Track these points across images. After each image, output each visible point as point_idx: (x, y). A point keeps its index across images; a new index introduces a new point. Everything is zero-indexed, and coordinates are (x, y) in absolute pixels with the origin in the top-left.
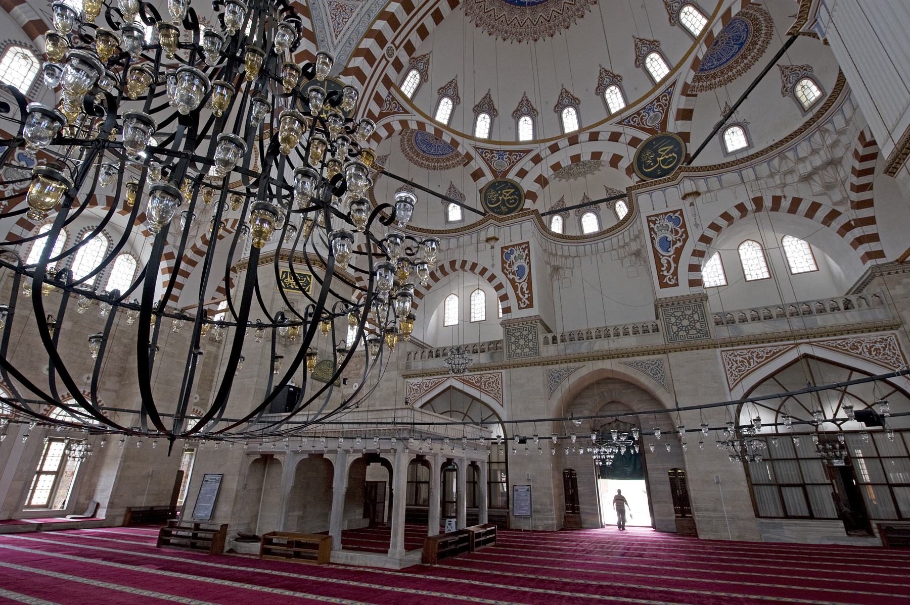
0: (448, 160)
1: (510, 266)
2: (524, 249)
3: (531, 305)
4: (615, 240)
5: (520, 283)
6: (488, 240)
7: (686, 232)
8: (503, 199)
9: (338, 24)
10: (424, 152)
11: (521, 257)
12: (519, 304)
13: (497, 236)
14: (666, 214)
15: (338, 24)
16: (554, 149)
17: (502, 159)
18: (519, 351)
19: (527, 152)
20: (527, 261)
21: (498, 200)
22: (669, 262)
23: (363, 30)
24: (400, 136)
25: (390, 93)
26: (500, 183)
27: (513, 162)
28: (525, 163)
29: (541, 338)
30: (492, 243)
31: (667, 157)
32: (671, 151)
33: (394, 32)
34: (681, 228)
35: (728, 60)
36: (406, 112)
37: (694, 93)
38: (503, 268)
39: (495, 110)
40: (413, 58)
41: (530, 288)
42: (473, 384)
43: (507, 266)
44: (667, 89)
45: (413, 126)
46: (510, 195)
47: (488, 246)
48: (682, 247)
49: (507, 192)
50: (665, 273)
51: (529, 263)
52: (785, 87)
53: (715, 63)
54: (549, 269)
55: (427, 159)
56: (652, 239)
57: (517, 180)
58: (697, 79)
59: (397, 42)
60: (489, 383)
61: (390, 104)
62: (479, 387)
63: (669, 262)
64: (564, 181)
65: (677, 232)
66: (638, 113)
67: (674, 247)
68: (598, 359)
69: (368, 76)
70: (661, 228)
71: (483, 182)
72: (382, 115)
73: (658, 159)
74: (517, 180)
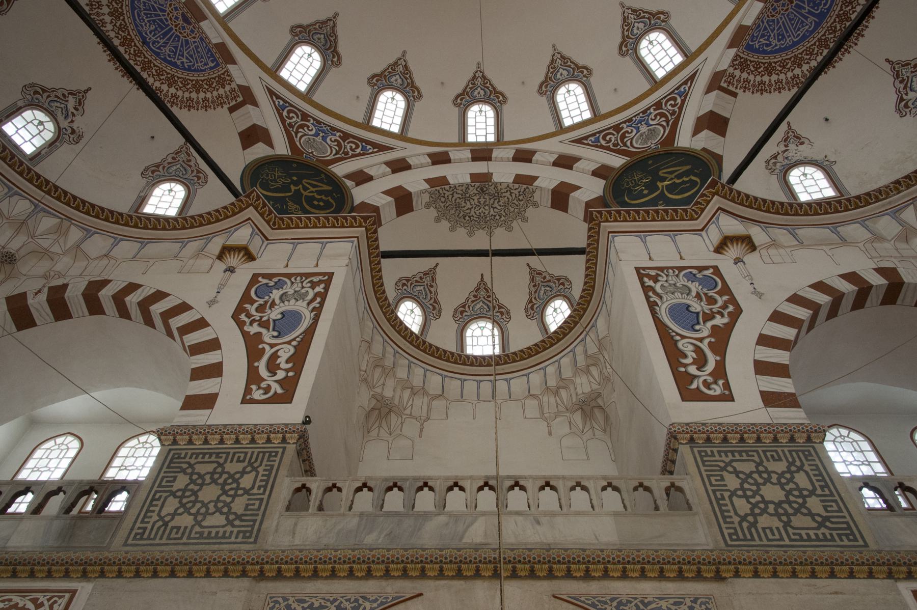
0: (197, 87)
1: (261, 309)
2: (313, 285)
3: (286, 397)
4: (536, 378)
5: (272, 346)
7: (733, 301)
8: (298, 192)
10: (145, 42)
11: (298, 296)
12: (248, 391)
13: (253, 249)
14: (681, 269)
16: (440, 159)
17: (324, 138)
18: (185, 521)
19: (382, 148)
20: (315, 304)
22: (698, 350)
27: (347, 153)
28: (372, 163)
29: (285, 486)
31: (678, 181)
32: (686, 173)
34: (721, 293)
35: (795, 44)
37: (731, 88)
39: (336, 53)
41: (299, 359)
43: (252, 309)
44: (677, 88)
47: (220, 266)
48: (730, 326)
50: (693, 370)
51: (318, 312)
52: (902, 100)
53: (774, 42)
54: (364, 399)
56: (652, 306)
58: (740, 63)
63: (698, 350)
64: (445, 224)
65: (711, 301)
66: (617, 128)
67: (709, 324)
68: (477, 575)
70: (672, 289)
71: (259, 151)
73: (660, 184)
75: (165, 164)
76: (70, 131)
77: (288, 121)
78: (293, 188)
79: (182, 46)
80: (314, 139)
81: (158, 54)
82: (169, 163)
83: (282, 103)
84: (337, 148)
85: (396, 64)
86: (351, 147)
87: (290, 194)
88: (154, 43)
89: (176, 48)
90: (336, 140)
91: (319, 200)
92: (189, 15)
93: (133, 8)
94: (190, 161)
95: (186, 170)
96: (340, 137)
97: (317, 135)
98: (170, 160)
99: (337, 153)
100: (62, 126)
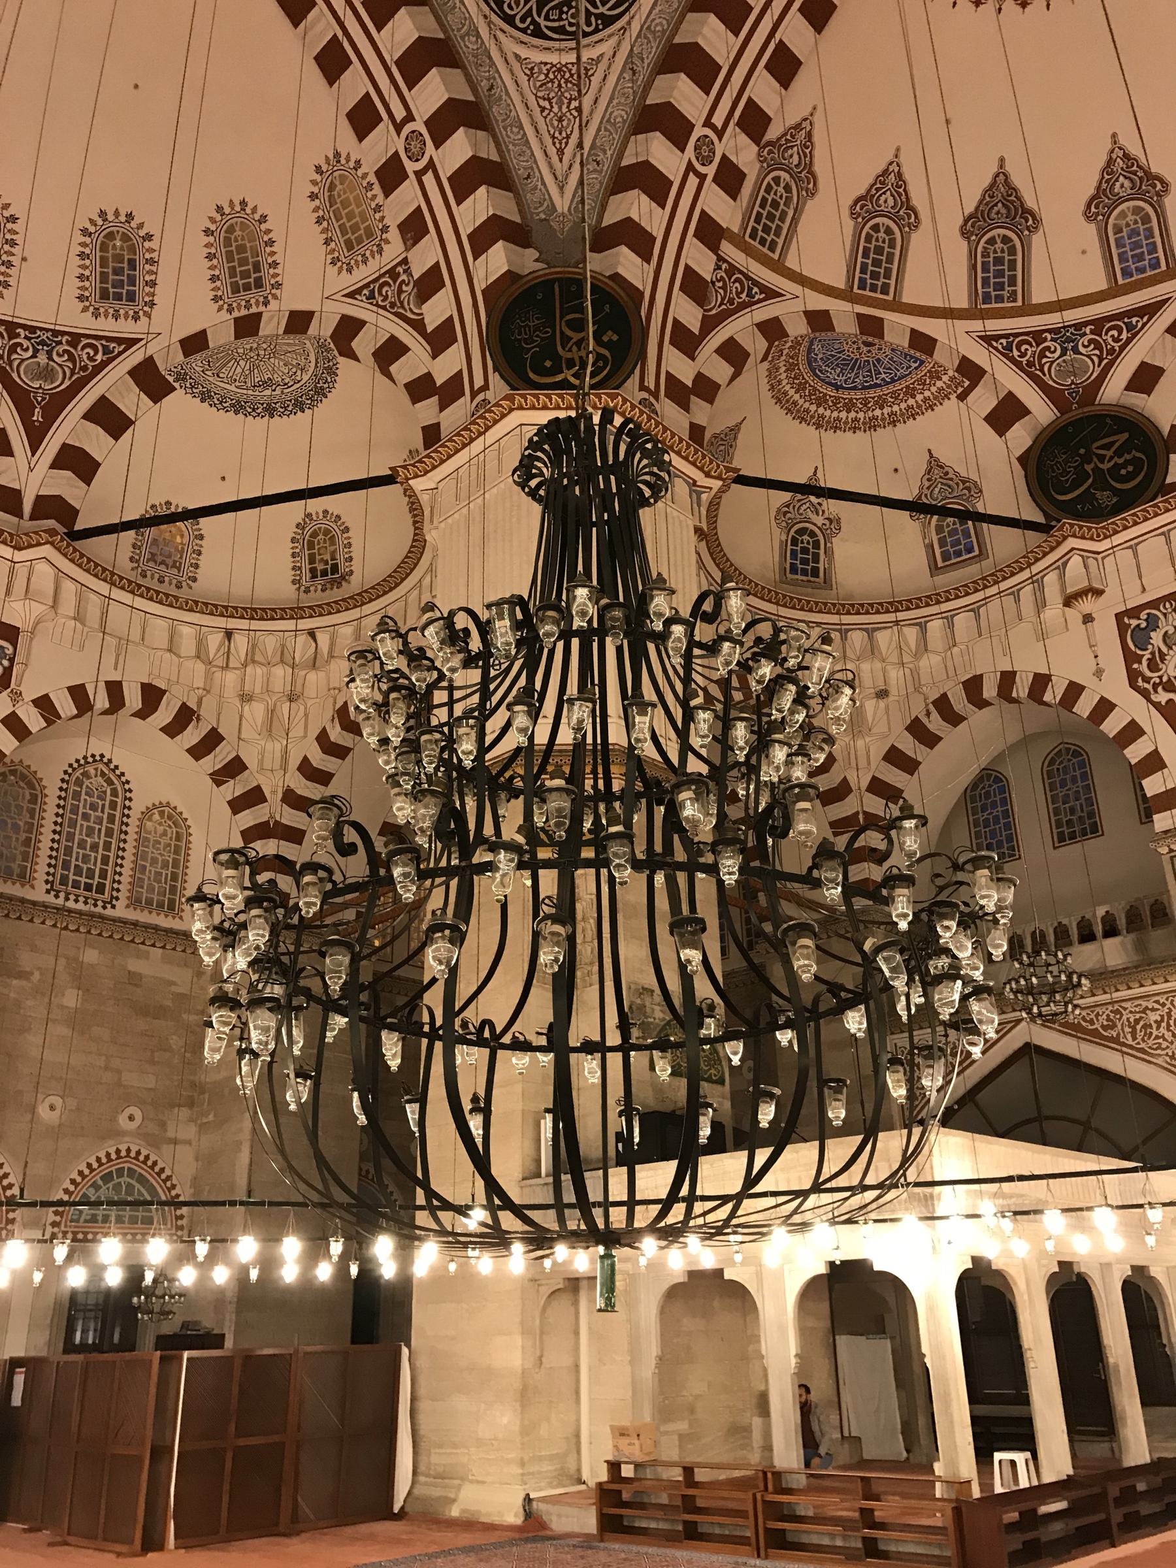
0: (911, 392)
6: (1068, 601)
8: (1096, 469)
9: (560, 120)
13: (1096, 585)
15: (560, 120)
17: (1076, 350)
21: (1082, 477)
23: (623, 114)
24: (766, 365)
25: (720, 259)
26: (1078, 424)
27: (1111, 351)
30: (1087, 605)
33: (707, 93)
36: (771, 294)
38: (1133, 677)
40: (769, 143)
42: (1095, 1033)
43: (1144, 667)
45: (797, 328)
46: (1119, 453)
47: (1074, 615)
49: (1107, 447)
55: (849, 406)
57: (1137, 400)
59: (718, 120)
60: (1145, 1026)
61: (724, 288)
62: (1116, 1040)
69: (659, 235)
72: (709, 324)
74: (1137, 400)
75: (925, 491)
76: (827, 522)
77: (1024, 360)
78: (1088, 468)
79: (875, 365)
80: (1064, 361)
81: (855, 388)
82: (928, 488)
83: (1004, 341)
84: (1097, 352)
85: (1110, 162)
86: (1112, 336)
87: (1090, 481)
88: (846, 381)
89: (870, 371)
90: (1090, 341)
91: (1124, 466)
92: (870, 339)
93: (813, 370)
94: (947, 473)
95: (949, 486)
96: (1092, 332)
97: (1063, 353)
98: (927, 484)
99: (1101, 360)
100: (820, 525)
